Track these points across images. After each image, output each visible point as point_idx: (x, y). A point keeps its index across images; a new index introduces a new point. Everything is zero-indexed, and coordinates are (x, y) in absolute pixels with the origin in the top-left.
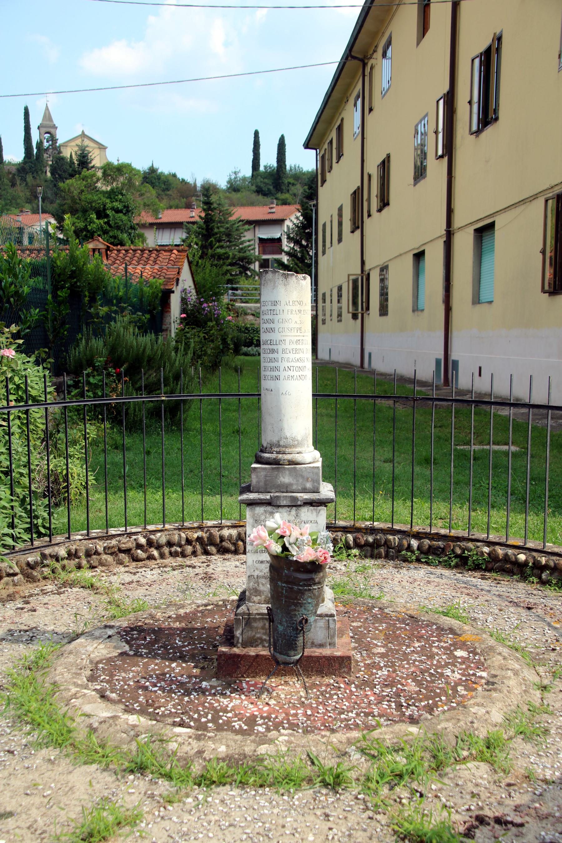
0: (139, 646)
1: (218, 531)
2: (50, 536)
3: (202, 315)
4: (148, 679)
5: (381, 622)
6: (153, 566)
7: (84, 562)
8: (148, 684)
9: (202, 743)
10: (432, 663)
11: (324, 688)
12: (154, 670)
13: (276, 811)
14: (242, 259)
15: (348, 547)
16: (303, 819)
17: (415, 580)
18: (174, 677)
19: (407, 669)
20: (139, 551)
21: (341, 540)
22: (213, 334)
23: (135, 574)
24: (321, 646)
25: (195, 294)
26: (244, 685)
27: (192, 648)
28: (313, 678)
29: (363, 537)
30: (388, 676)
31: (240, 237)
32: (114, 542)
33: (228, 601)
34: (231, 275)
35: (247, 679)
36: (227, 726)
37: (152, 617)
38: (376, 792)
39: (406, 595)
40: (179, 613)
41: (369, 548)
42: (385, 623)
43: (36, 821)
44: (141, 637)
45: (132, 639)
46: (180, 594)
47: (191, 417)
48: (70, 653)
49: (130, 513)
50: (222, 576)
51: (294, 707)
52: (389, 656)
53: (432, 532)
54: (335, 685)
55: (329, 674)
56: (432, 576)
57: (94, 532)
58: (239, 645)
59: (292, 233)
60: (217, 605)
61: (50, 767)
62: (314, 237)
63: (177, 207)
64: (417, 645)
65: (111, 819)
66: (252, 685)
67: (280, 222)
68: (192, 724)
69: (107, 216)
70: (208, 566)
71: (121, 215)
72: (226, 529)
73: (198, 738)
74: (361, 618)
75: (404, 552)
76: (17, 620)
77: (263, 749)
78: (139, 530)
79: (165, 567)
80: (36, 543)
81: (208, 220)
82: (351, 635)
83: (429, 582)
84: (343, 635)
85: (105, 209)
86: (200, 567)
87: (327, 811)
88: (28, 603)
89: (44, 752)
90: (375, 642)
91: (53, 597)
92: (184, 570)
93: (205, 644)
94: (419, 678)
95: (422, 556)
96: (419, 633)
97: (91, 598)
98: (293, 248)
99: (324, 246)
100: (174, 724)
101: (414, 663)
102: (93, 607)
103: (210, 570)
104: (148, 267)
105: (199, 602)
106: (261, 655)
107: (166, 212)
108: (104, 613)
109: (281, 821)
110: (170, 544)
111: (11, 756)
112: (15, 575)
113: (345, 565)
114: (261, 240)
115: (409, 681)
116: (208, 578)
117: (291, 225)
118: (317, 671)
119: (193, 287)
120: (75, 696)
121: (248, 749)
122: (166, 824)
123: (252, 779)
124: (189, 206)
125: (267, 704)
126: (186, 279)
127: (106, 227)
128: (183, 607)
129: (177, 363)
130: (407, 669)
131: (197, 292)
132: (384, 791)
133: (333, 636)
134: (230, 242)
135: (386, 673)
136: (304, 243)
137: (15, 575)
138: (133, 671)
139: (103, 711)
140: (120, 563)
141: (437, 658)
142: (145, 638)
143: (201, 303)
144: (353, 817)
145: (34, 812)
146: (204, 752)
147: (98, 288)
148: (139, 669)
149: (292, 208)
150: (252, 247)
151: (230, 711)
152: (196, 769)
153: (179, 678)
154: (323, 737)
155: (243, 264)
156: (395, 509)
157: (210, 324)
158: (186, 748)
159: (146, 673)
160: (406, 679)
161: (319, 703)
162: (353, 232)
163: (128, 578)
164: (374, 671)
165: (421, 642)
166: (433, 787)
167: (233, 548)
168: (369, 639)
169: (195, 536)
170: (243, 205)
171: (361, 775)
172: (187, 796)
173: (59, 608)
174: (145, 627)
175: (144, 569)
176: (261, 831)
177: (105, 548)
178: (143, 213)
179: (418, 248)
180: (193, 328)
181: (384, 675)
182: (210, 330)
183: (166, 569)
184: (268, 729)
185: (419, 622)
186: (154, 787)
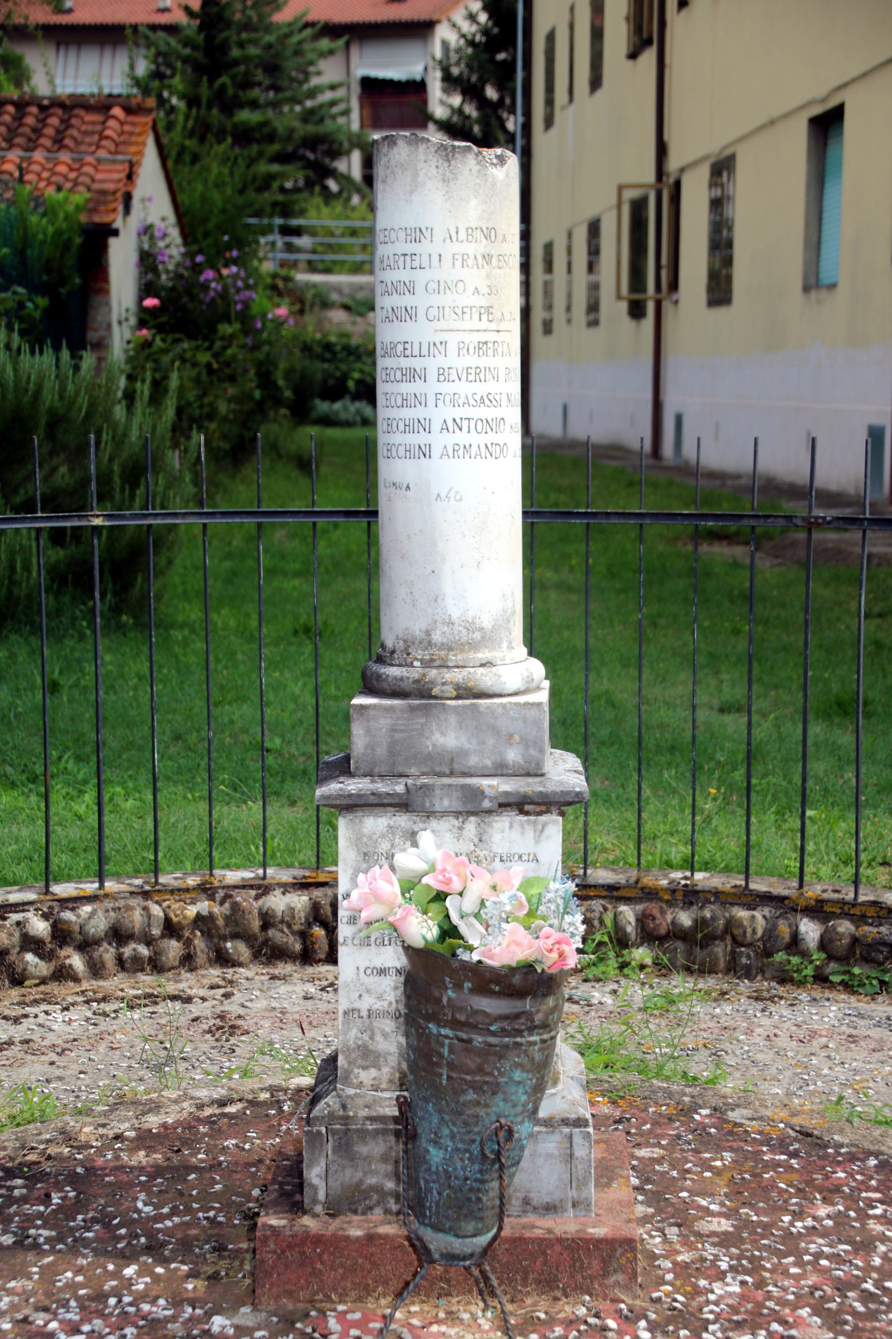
0: (29, 1220)
1: (257, 898)
3: (201, 302)
4: (55, 1314)
5: (719, 1149)
6: (70, 999)
8: (53, 1325)
10: (867, 1262)
12: (72, 1286)
14: (312, 142)
15: (621, 942)
17: (813, 1034)
18: (131, 1304)
19: (797, 1278)
20: (29, 957)
21: (602, 922)
22: (234, 357)
23: (16, 1021)
24: (550, 1208)
25: (179, 240)
26: (333, 1323)
27: (183, 1224)
28: (529, 1301)
29: (663, 913)
30: (743, 1297)
31: (307, 76)
33: (286, 1090)
34: (282, 190)
35: (341, 1308)
37: (67, 1137)
39: (788, 1073)
40: (146, 1126)
41: (680, 946)
42: (731, 1149)
44: (36, 1193)
46: (147, 1075)
47: (175, 585)
50: (267, 1024)
52: (742, 1241)
53: (862, 898)
54: (592, 1320)
56: (862, 1022)
58: (318, 1209)
59: (458, 64)
62: (520, 75)
64: (823, 1211)
66: (355, 1324)
67: (421, 29)
70: (227, 996)
72: (278, 892)
74: (663, 1136)
75: (780, 956)
78: (31, 896)
79: (104, 999)
82: (635, 1181)
83: (853, 1039)
84: (611, 1180)
86: (204, 999)
90: (704, 1203)
92: (160, 1008)
93: (219, 1210)
94: (833, 1306)
95: (833, 966)
96: (827, 1177)
98: (460, 111)
99: (550, 102)
101: (815, 1263)
103: (232, 1007)
105: (203, 1094)
106: (380, 1236)
110: (119, 935)
113: (615, 992)
114: (370, 86)
115: (804, 1312)
116: (226, 1028)
117: (453, 38)
118: (538, 1282)
119: (172, 219)
126: (152, 200)
128: (155, 1107)
129: (134, 435)
130: (790, 1280)
131: (184, 234)
133: (582, 1183)
134: (277, 89)
135: (737, 1289)
136: (491, 93)
138: (10, 1292)
141: (882, 1248)
142: (48, 1196)
143: (197, 269)
148: (30, 1285)
150: (341, 107)
153: (146, 1307)
155: (315, 155)
156: (753, 838)
157: (225, 329)
159: (48, 1294)
160: (795, 1307)
162: (633, 56)
164: (702, 1283)
165: (833, 1204)
167: (298, 947)
168: (684, 1194)
169: (192, 911)
174: (47, 1167)
175: (44, 1007)
179: (824, 100)
180: (177, 341)
181: (731, 1294)
182: (225, 348)
183: (108, 1007)
185: (826, 1147)
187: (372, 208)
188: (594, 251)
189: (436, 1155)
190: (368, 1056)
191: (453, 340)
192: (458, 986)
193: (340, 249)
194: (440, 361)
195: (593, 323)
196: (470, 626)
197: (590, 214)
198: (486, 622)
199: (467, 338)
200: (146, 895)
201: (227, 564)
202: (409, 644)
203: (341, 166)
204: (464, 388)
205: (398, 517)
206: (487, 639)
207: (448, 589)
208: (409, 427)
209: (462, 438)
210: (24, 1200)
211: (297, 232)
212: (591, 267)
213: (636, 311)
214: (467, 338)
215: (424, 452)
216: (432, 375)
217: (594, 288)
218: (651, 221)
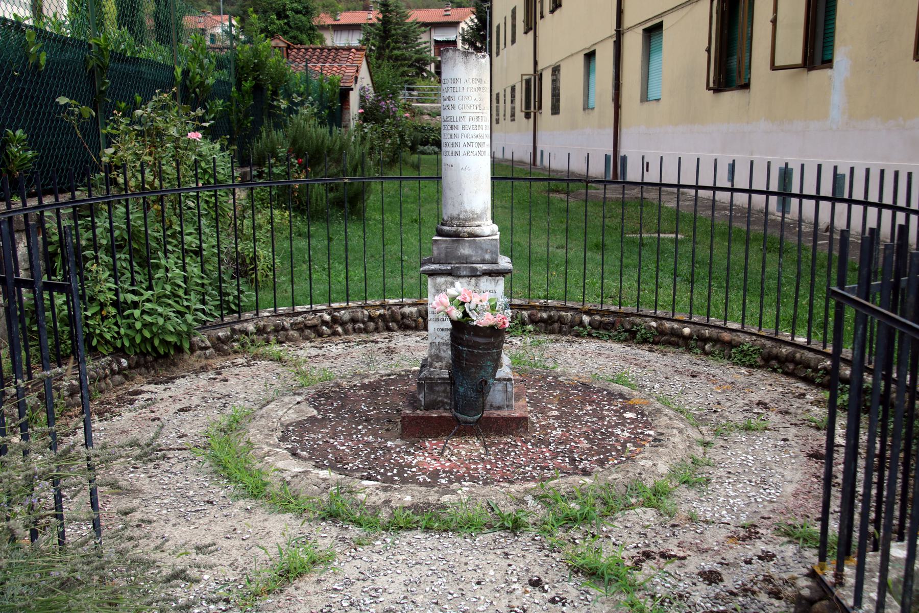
2: (239, 313)
7: (272, 337)
9: (388, 494)
11: (502, 446)
12: (341, 432)
13: (459, 551)
14: (418, 61)
16: (484, 558)
20: (324, 328)
23: (320, 348)
26: (427, 444)
31: (417, 39)
32: (300, 319)
36: (413, 480)
37: (339, 386)
38: (551, 535)
43: (237, 560)
45: (320, 405)
48: (262, 417)
49: (316, 292)
51: (475, 463)
55: (506, 434)
57: (281, 309)
60: (399, 375)
61: (247, 515)
63: (355, 10)
65: (306, 558)
66: (434, 444)
68: (379, 477)
69: (287, 17)
71: (300, 16)
73: (385, 489)
76: (210, 388)
77: (446, 498)
78: (324, 307)
80: (226, 319)
81: (385, 22)
85: (284, 10)
87: (506, 550)
88: (220, 374)
89: (241, 502)
91: (242, 369)
97: (279, 370)
99: (498, 48)
100: (362, 478)
102: (282, 378)
103: (392, 345)
104: (327, 65)
105: (383, 372)
107: (344, 14)
108: (291, 382)
109: (464, 560)
110: (354, 320)
111: (210, 506)
112: (207, 348)
116: (390, 351)
120: (268, 454)
121: (432, 498)
122: (358, 563)
123: (437, 524)
124: (366, 8)
125: (449, 460)
127: (286, 27)
128: (367, 376)
132: (559, 533)
134: (407, 43)
137: (207, 348)
138: (322, 433)
139: (294, 467)
140: (307, 339)
143: (379, 101)
144: (530, 555)
145: (234, 552)
146: (390, 501)
147: (280, 83)
149: (467, 10)
151: (415, 467)
152: (384, 515)
154: (502, 487)
158: (374, 498)
159: (334, 434)
161: (497, 459)
162: (526, 33)
163: (314, 352)
166: (604, 529)
169: (378, 313)
170: (418, 8)
171: (537, 520)
172: (377, 539)
173: (249, 378)
176: (446, 567)
177: (292, 324)
178: (322, 15)
184: (450, 482)
186: (345, 532)
187: (440, 82)
188: (513, 96)
189: (461, 390)
190: (438, 358)
191: (467, 116)
192: (469, 334)
193: (428, 95)
194: (463, 123)
195: (513, 120)
196: (473, 213)
197: (512, 84)
198: (479, 212)
199: (472, 115)
200: (363, 307)
201: (388, 199)
202: (452, 219)
203: (428, 68)
204: (471, 132)
205: (448, 175)
206: (479, 217)
207: (465, 200)
208: (452, 145)
209: (470, 149)
210: (324, 405)
211: (413, 90)
212: (512, 102)
213: (528, 116)
214: (472, 115)
215: (458, 154)
216: (460, 128)
217: (513, 109)
218: (532, 87)
